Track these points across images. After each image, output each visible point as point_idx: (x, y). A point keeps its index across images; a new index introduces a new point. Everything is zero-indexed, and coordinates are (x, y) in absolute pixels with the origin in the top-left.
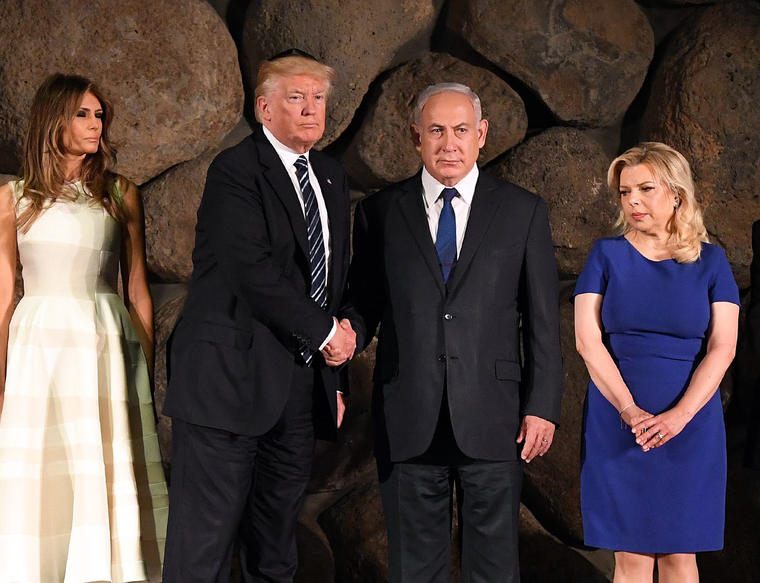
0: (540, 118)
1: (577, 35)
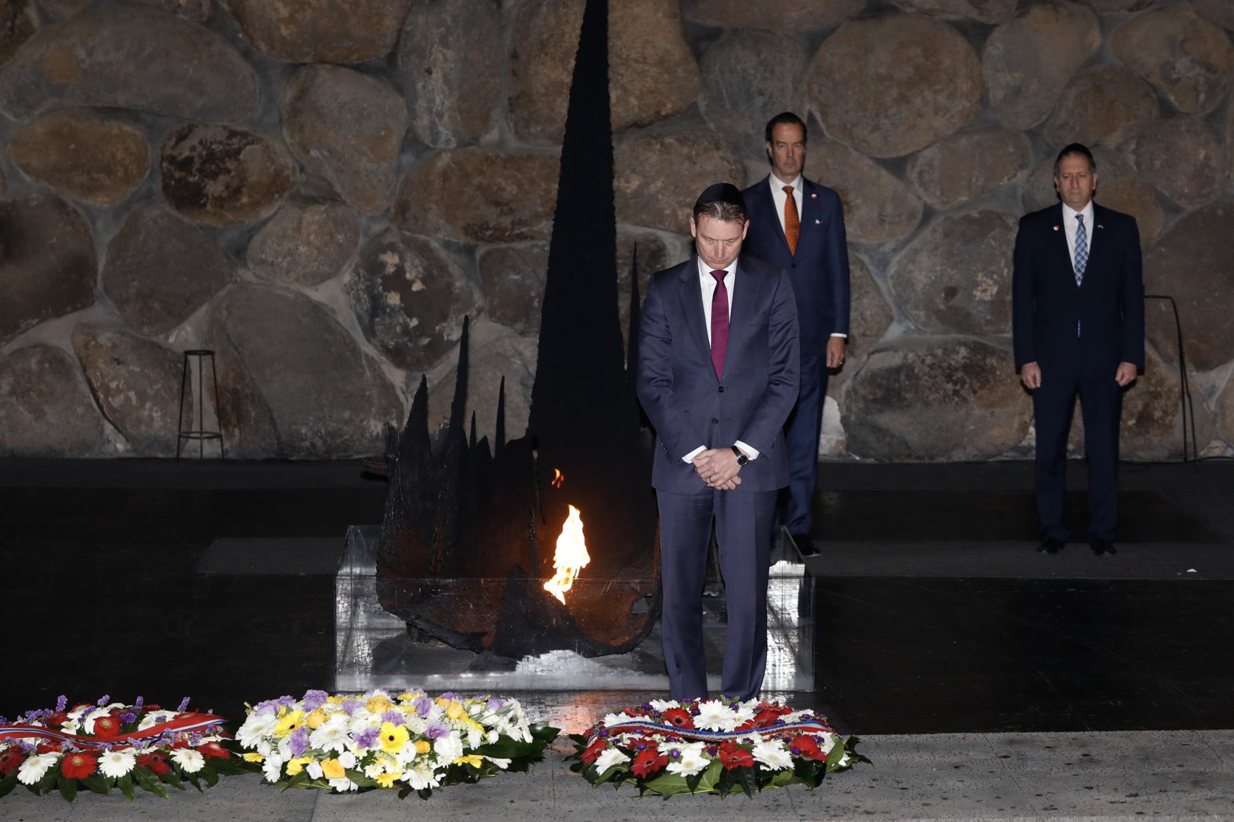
0: (1167, 112)
1: (1193, 61)
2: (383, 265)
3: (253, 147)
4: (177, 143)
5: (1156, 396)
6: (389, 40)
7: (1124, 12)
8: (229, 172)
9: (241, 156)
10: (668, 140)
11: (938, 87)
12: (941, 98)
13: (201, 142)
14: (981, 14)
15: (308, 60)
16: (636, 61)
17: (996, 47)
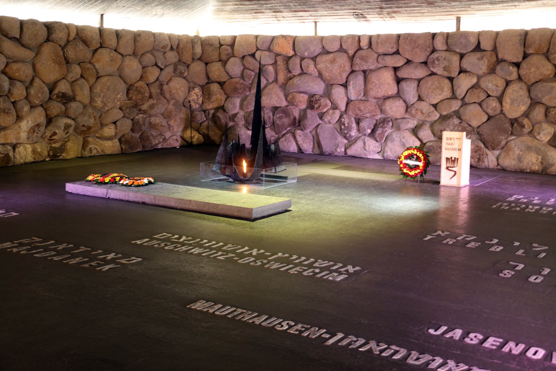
17: (455, 81)
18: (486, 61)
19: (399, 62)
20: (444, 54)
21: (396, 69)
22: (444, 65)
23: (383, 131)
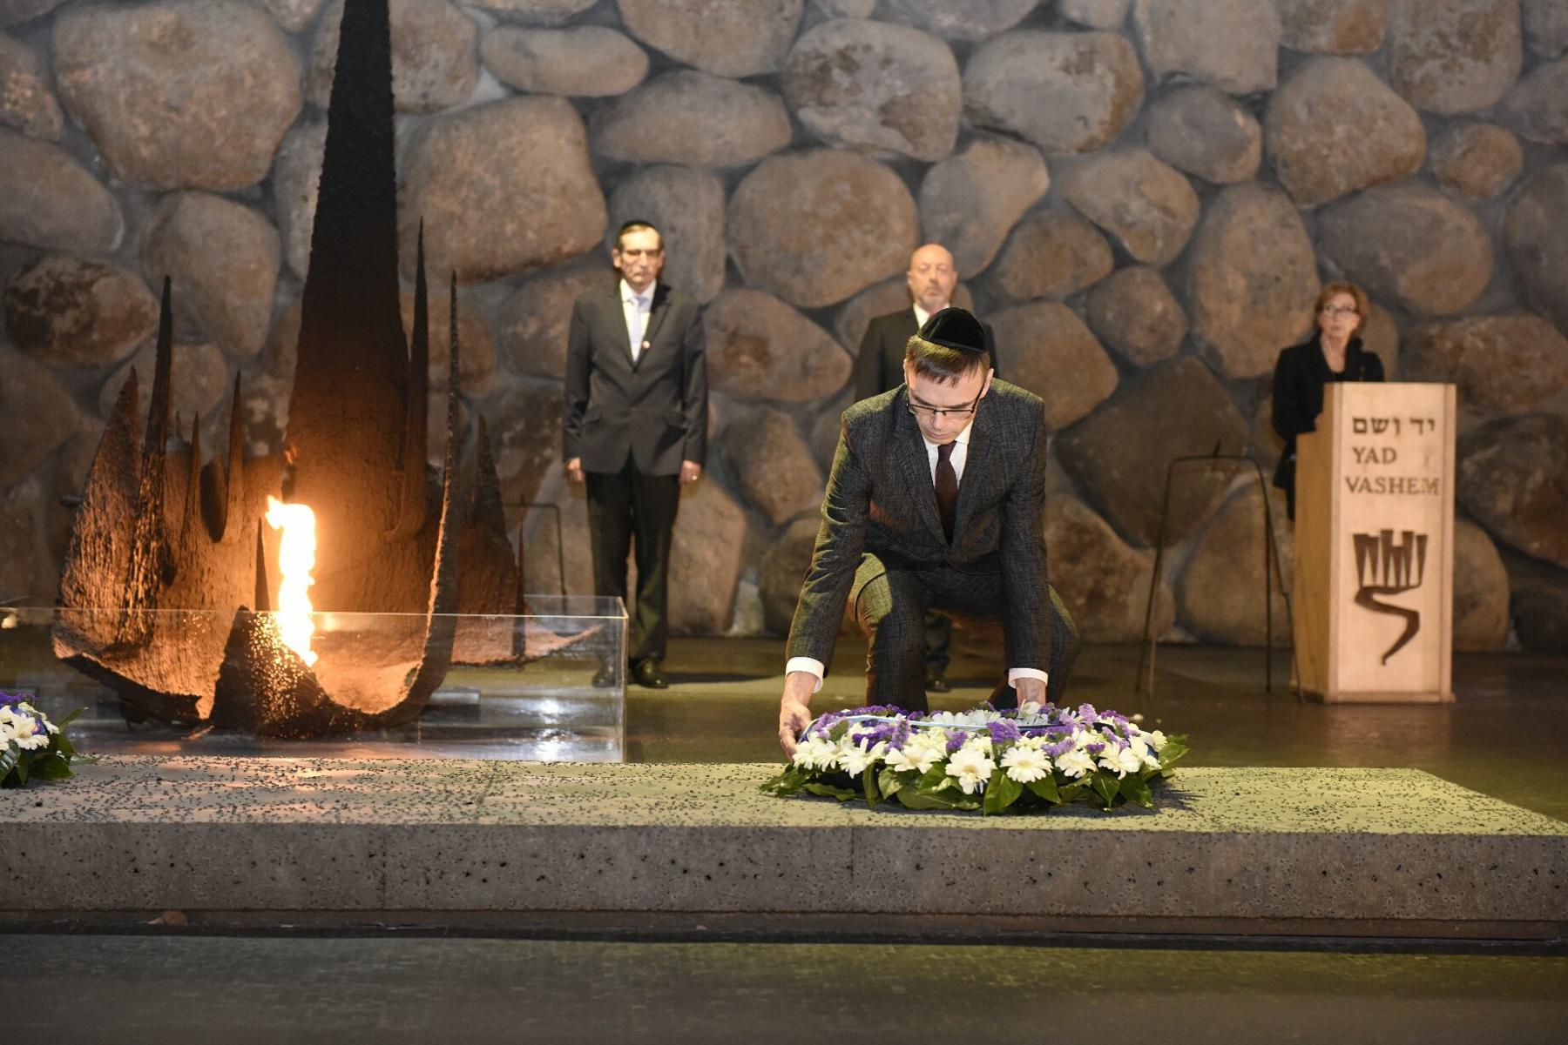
0: (1122, 260)
1: (1150, 203)
2: (251, 412)
3: (108, 280)
4: (22, 274)
5: (1108, 572)
6: (264, 165)
7: (1074, 153)
8: (77, 305)
9: (94, 289)
10: (569, 281)
11: (868, 227)
12: (871, 240)
13: (48, 273)
14: (916, 149)
15: (170, 184)
16: (535, 191)
17: (933, 186)
18: (1110, 81)
19: (604, 63)
20: (878, 36)
21: (593, 112)
22: (882, 96)
23: (528, 464)
